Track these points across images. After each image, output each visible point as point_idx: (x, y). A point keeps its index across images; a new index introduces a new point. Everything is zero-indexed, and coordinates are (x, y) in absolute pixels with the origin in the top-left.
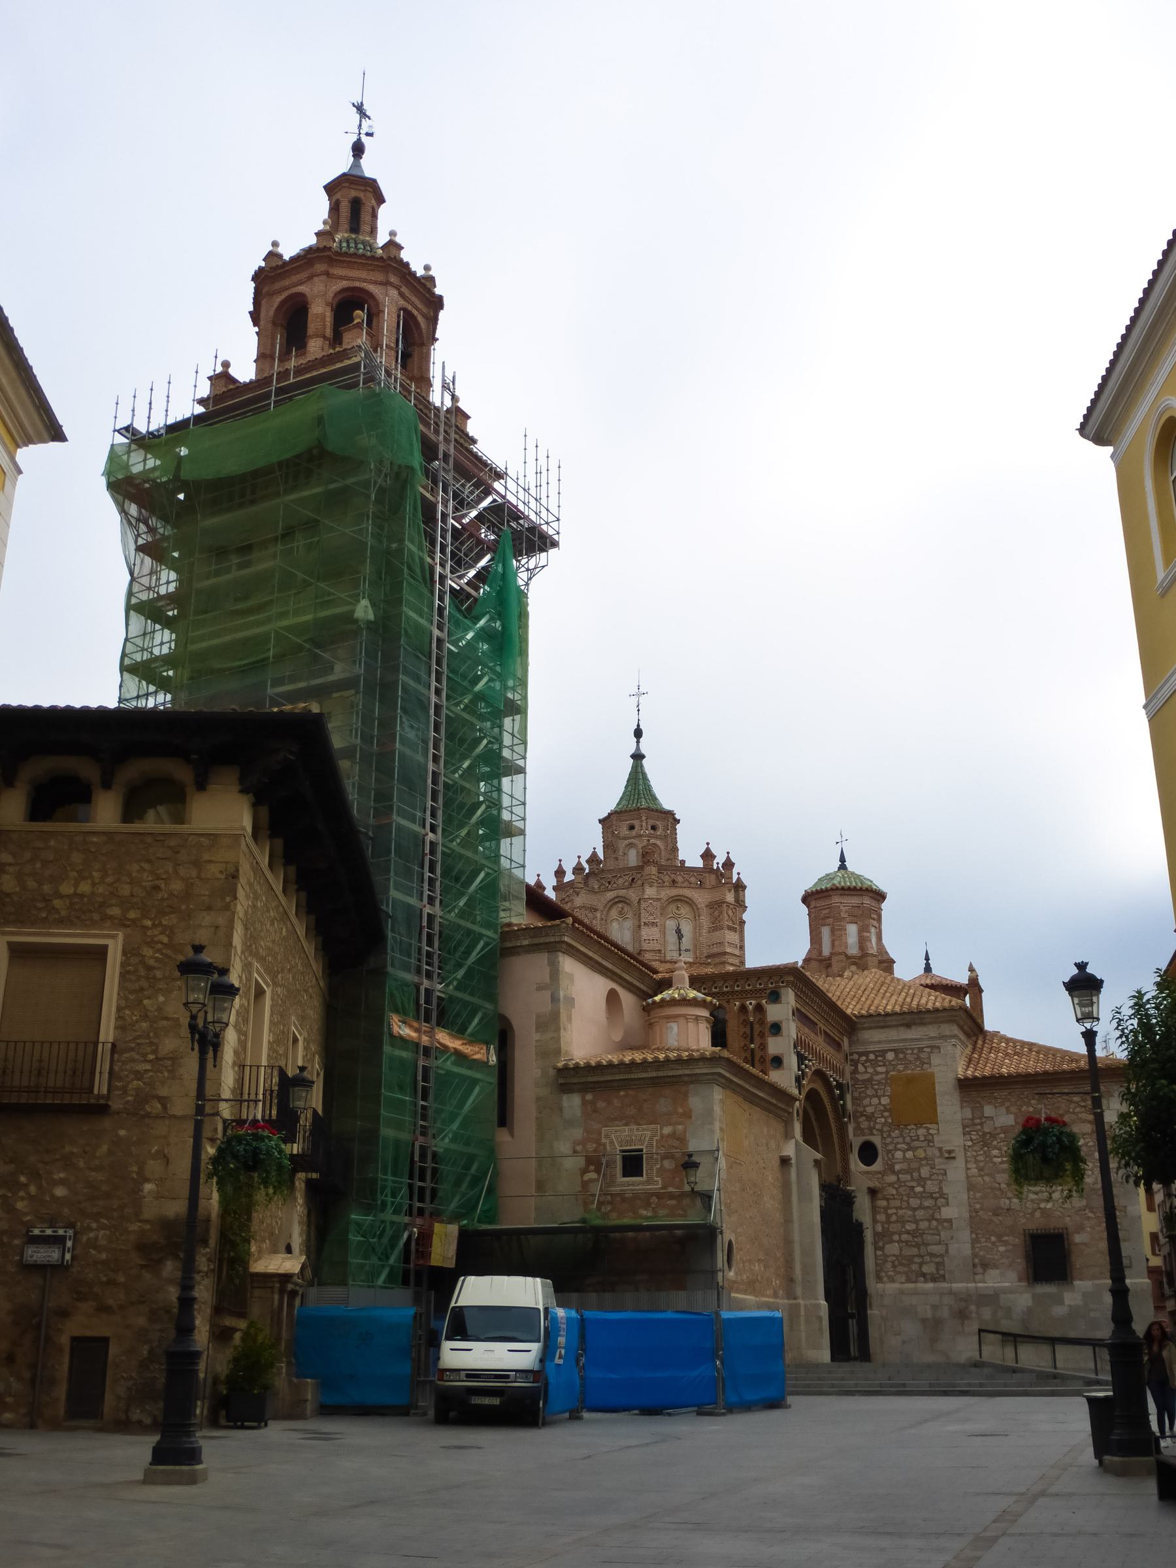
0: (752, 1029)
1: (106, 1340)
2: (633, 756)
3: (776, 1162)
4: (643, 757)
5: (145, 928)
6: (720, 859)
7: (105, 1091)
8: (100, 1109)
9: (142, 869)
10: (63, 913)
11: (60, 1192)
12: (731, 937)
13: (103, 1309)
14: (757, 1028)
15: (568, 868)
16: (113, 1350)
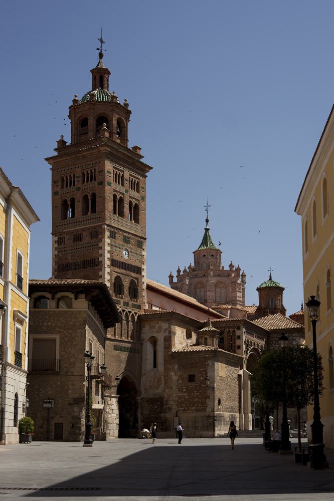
0: (232, 337)
1: (62, 423)
2: (205, 229)
3: (236, 376)
4: (209, 229)
5: (65, 333)
6: (236, 266)
7: (58, 370)
8: (58, 374)
9: (63, 319)
10: (45, 330)
11: (50, 392)
12: (239, 294)
13: (61, 417)
14: (233, 337)
15: (182, 270)
16: (64, 425)
